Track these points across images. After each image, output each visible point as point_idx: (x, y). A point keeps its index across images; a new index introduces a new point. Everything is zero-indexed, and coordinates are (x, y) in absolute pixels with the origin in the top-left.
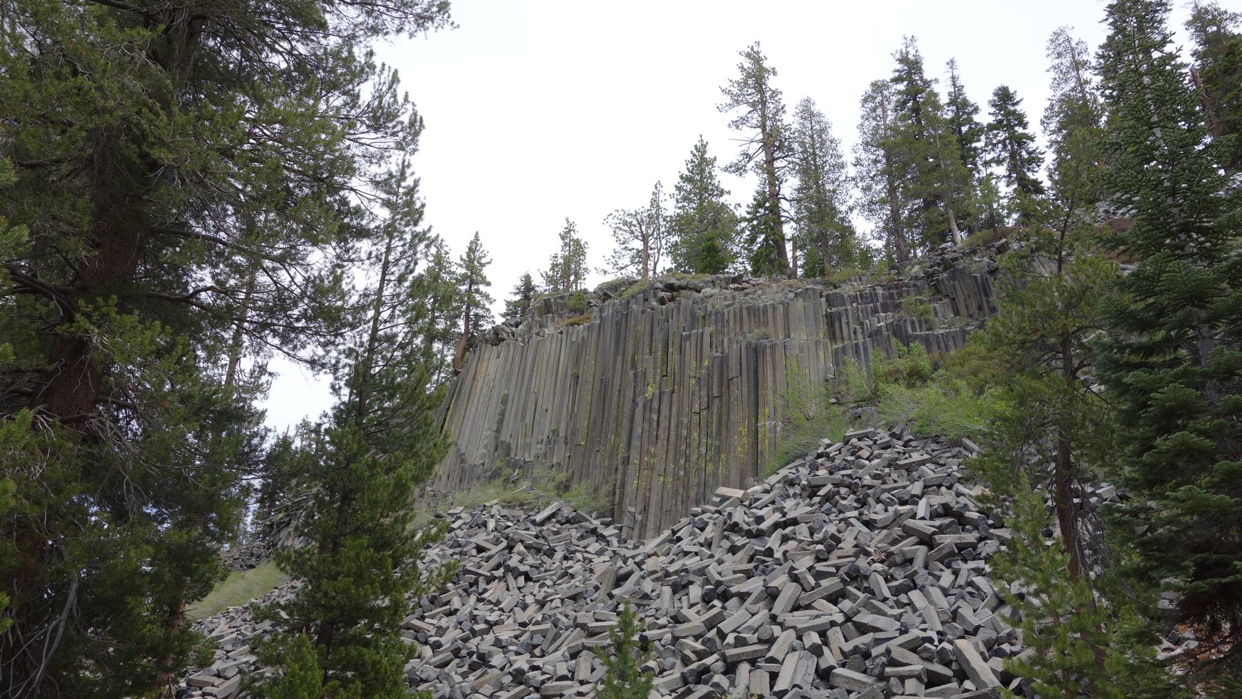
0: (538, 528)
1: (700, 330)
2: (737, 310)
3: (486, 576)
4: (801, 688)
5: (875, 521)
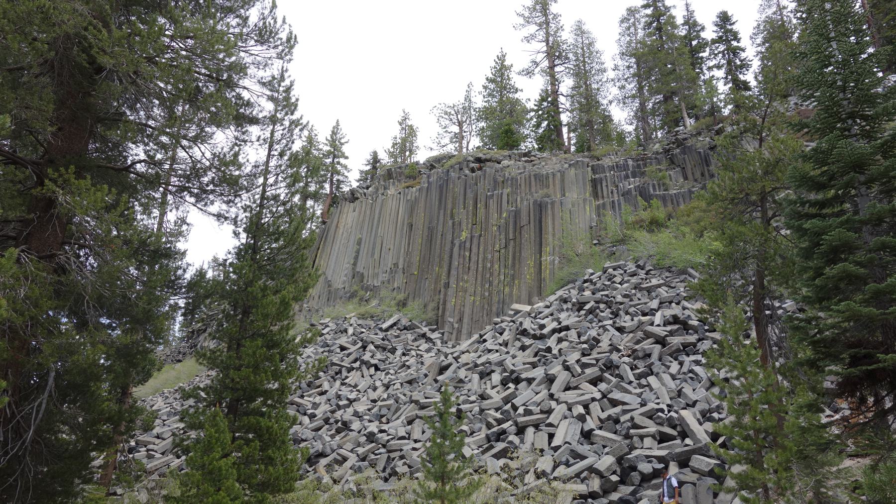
0: (384, 333)
1: (500, 191)
2: (527, 176)
3: (347, 367)
4: (570, 444)
5: (624, 327)
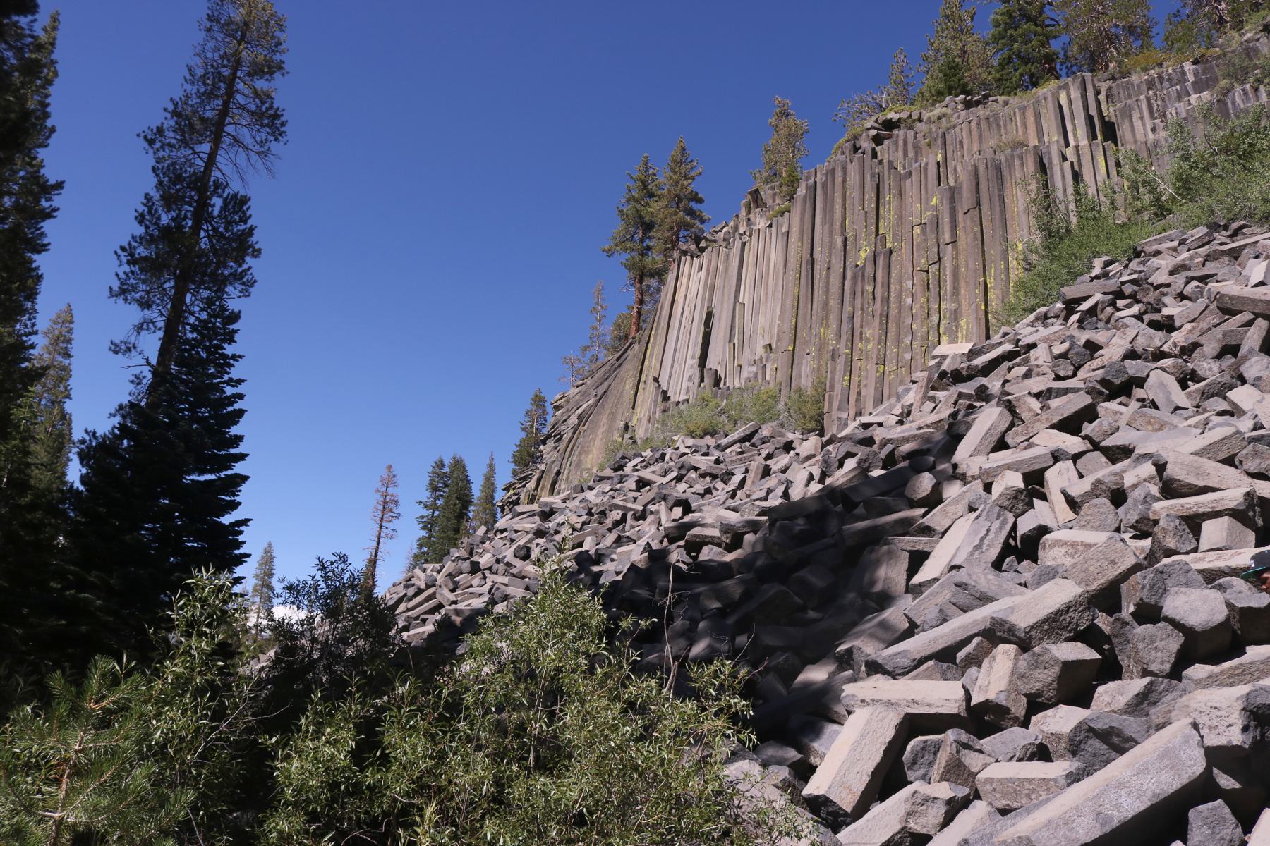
5: (1171, 318)
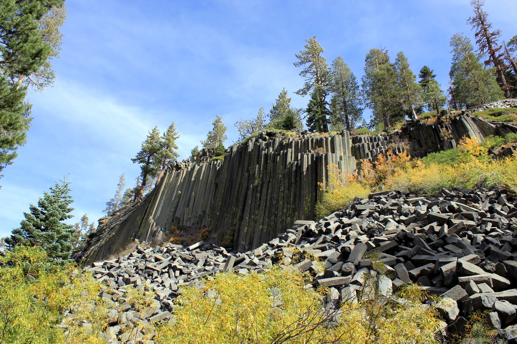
1: (285, 151)
